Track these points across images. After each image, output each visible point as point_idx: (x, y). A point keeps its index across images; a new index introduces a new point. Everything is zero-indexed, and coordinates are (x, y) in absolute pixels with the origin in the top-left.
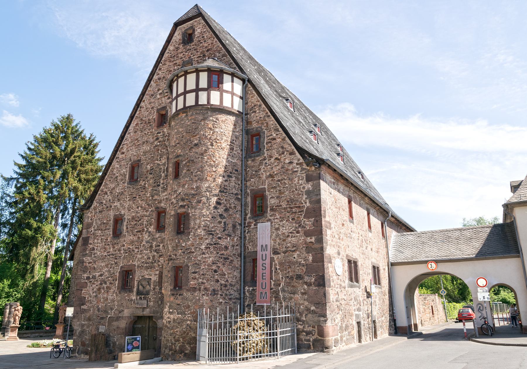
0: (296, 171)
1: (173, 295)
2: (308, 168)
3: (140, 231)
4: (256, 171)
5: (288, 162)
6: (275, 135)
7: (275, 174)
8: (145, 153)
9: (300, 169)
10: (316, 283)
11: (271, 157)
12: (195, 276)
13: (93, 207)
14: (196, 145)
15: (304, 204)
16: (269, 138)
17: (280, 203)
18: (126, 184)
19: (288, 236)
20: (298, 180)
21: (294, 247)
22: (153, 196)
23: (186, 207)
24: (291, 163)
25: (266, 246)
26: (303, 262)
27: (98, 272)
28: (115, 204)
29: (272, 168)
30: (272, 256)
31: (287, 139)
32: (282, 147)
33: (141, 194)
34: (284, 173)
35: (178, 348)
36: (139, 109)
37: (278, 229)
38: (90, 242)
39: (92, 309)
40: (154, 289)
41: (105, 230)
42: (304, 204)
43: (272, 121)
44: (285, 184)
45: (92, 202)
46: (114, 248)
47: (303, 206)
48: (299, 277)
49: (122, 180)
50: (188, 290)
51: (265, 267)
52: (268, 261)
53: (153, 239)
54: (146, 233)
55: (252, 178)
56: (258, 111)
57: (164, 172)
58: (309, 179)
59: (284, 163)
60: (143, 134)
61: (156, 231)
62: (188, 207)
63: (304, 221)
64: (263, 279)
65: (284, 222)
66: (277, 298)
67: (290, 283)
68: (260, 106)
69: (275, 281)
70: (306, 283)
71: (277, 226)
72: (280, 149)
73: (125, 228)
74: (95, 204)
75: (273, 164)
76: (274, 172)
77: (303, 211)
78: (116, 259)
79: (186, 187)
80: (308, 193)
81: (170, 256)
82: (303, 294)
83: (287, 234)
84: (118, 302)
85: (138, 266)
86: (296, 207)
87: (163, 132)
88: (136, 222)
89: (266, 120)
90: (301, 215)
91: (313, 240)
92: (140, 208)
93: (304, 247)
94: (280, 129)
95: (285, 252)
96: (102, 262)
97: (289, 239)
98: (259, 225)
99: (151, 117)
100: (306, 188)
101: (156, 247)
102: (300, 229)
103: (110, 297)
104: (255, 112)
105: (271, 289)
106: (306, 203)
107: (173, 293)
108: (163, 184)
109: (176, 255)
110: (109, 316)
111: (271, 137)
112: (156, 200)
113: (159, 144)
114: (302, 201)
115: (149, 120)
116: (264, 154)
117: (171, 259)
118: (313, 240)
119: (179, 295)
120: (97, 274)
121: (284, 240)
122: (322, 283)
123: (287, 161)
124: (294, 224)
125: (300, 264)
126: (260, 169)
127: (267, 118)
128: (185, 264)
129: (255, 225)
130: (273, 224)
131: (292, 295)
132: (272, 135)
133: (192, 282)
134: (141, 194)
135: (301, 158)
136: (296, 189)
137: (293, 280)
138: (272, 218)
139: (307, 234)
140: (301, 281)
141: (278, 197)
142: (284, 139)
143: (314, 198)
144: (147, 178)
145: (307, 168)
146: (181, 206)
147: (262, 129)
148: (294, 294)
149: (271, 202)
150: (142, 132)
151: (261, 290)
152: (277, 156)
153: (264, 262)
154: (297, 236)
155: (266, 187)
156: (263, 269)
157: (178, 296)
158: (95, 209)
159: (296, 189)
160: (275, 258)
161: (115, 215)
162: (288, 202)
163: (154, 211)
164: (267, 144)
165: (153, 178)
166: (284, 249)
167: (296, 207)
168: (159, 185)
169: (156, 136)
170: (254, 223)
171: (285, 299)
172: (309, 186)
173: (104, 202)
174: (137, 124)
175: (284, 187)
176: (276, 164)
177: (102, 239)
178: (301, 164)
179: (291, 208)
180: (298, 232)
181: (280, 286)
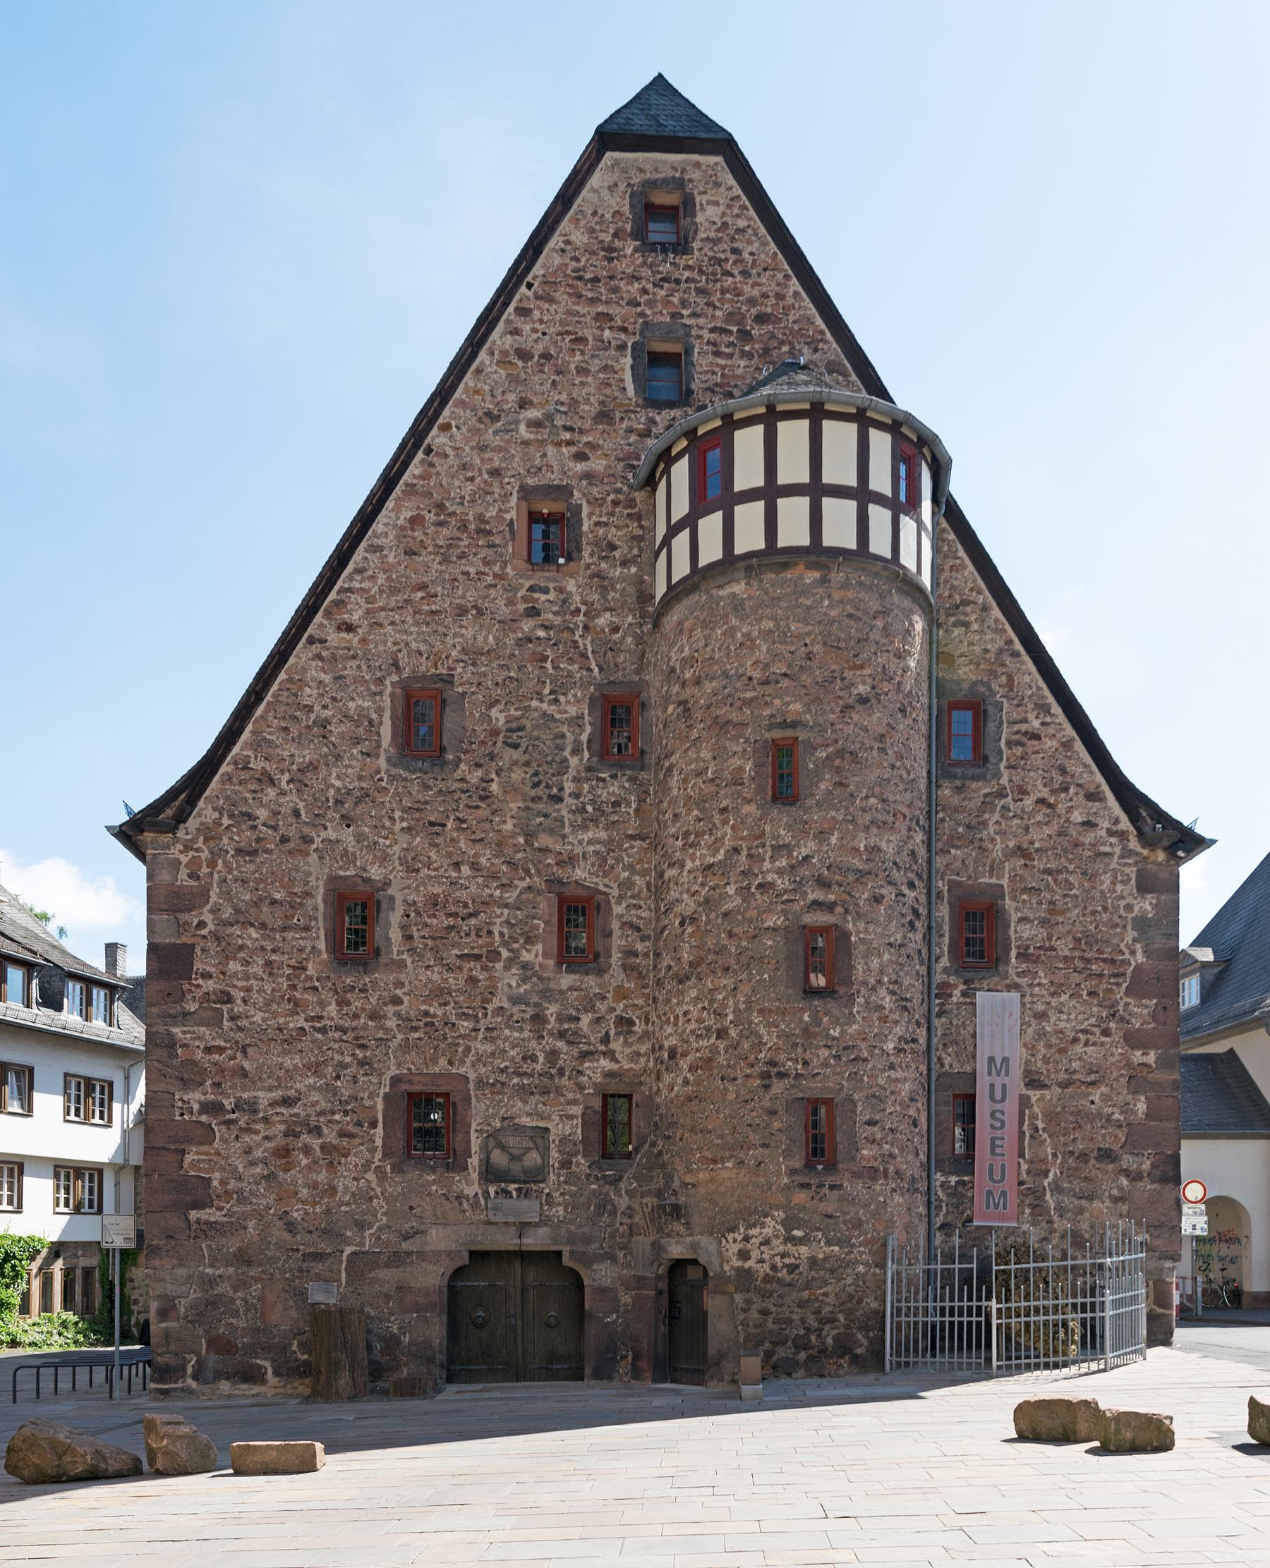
0: (1107, 854)
2: (1145, 852)
3: (477, 957)
4: (969, 827)
5: (1080, 820)
6: (1036, 724)
7: (1037, 850)
8: (472, 654)
9: (1118, 850)
10: (1157, 1173)
11: (1022, 791)
12: (873, 1134)
13: (192, 823)
15: (1127, 956)
16: (1016, 728)
17: (1050, 939)
18: (382, 762)
19: (1075, 1040)
20: (1113, 883)
21: (1091, 1072)
22: (530, 836)
24: (1089, 825)
25: (1005, 1060)
26: (1116, 1116)
27: (270, 1089)
28: (331, 834)
29: (1027, 829)
30: (1024, 1091)
31: (1079, 746)
32: (1063, 770)
33: (471, 816)
34: (1065, 850)
36: (420, 455)
37: (1042, 1016)
38: (198, 966)
39: (251, 1224)
40: (566, 1164)
41: (284, 929)
42: (1127, 956)
44: (1070, 886)
45: (192, 802)
46: (342, 1003)
47: (1123, 961)
48: (1106, 1155)
49: (356, 741)
51: (1003, 1123)
52: (1010, 1107)
53: (547, 994)
54: (507, 968)
55: (957, 847)
56: (975, 627)
57: (576, 751)
58: (1145, 885)
59: (1067, 820)
61: (559, 964)
63: (1127, 1004)
64: (993, 1153)
65: (1064, 998)
66: (1038, 1207)
67: (1077, 1169)
68: (985, 608)
69: (1031, 1162)
70: (1127, 1173)
71: (1040, 1007)
73: (395, 935)
74: (205, 812)
75: (1031, 815)
76: (1032, 843)
77: (1124, 974)
78: (363, 1047)
80: (1141, 924)
82: (1115, 1200)
83: (1071, 1035)
84: (391, 1200)
85: (481, 1083)
86: (1104, 961)
87: (561, 590)
88: (451, 921)
89: (1004, 665)
90: (1119, 985)
91: (1151, 1058)
92: (466, 870)
93: (1122, 1075)
94: (1056, 709)
95: (1059, 1085)
96: (285, 1053)
97: (1079, 1049)
98: (980, 995)
99: (492, 512)
100: (1136, 908)
101: (560, 1020)
102: (1112, 1025)
103: (345, 1182)
104: (967, 625)
105: (1021, 1183)
106: (1133, 953)
108: (576, 795)
110: (348, 1250)
111: (1024, 727)
112: (545, 851)
113: (541, 633)
114: (1122, 946)
115: (480, 518)
116: (998, 775)
118: (1151, 1058)
120: (264, 1098)
121: (1062, 1051)
122: (1171, 1174)
123: (1077, 817)
124: (1095, 1009)
125: (1108, 1120)
126: (984, 824)
127: (1008, 660)
128: (844, 1094)
129: (964, 994)
130: (1028, 999)
131: (1084, 1203)
132: (1025, 721)
133: (865, 1152)
134: (471, 816)
135: (1124, 818)
136: (1105, 909)
137: (1087, 1162)
138: (1023, 981)
139: (1134, 1040)
140: (1111, 1167)
141: (1043, 922)
142: (1067, 745)
143: (1159, 943)
144: (492, 757)
145: (1139, 849)
147: (993, 694)
148: (1090, 1198)
149: (1021, 931)
150: (446, 560)
151: (989, 1185)
152: (1044, 793)
153: (998, 1107)
154: (1103, 1044)
155: (1005, 882)
156: (992, 1127)
158: (209, 833)
159: (1105, 909)
160: (1033, 1099)
161: (333, 879)
162: (1078, 940)
163: (539, 892)
164: (1009, 744)
165: (527, 764)
166: (1062, 1076)
167: (1104, 961)
168: (558, 799)
170: (962, 987)
171: (1061, 1210)
172: (1146, 905)
173: (263, 814)
174: (416, 521)
175: (1065, 896)
176: (1039, 818)
177: (269, 964)
178: (1122, 835)
179: (1088, 961)
180: (1106, 1032)
181: (1047, 1176)
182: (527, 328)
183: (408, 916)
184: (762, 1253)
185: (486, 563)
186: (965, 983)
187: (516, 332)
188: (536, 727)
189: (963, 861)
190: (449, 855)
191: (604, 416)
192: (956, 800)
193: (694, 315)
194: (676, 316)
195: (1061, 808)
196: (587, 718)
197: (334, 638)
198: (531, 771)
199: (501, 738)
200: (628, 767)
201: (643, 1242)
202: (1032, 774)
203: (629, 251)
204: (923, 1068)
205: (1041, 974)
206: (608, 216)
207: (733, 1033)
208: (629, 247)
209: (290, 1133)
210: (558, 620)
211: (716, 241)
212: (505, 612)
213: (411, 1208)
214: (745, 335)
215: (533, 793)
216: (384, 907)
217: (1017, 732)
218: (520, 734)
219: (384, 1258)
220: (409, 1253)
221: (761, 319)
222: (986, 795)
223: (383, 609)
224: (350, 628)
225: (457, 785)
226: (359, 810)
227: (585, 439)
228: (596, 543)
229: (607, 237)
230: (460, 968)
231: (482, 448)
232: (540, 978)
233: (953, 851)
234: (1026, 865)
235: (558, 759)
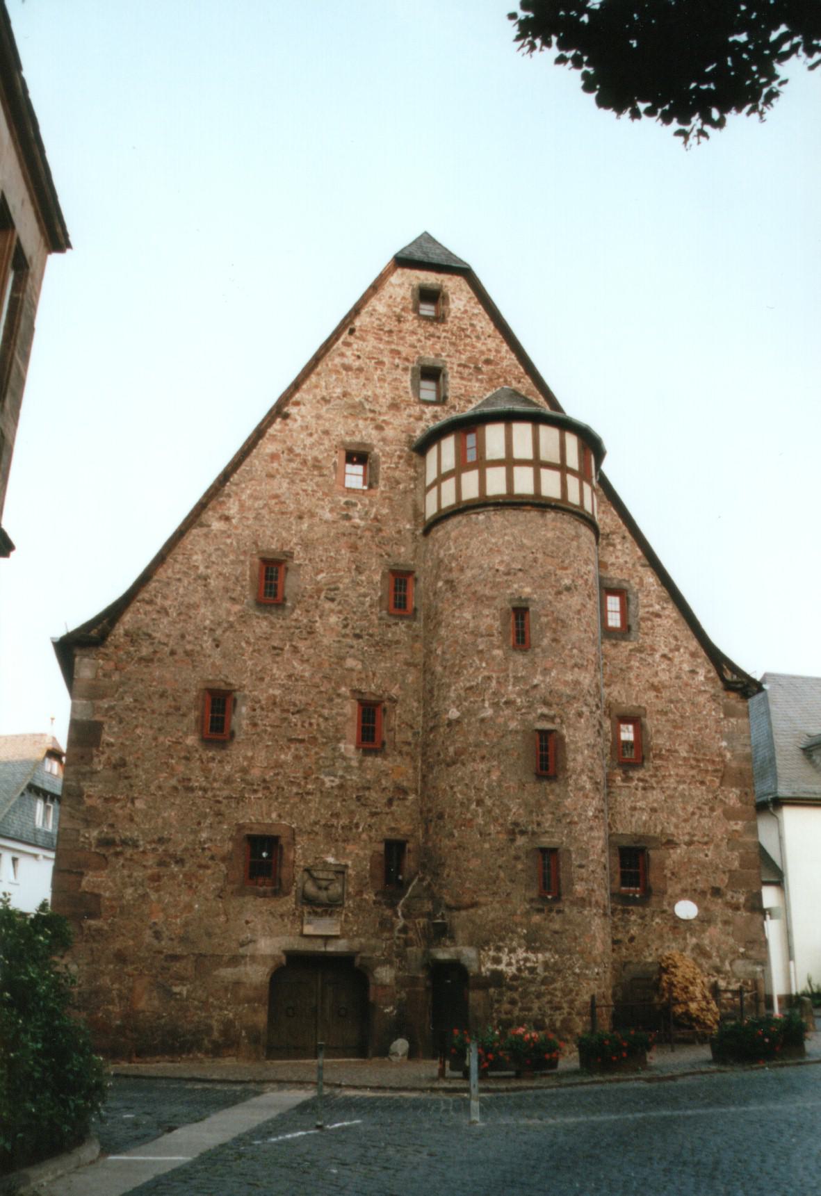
1: (540, 911)
3: (302, 741)
11: (653, 650)
14: (568, 589)
23: (558, 720)
24: (693, 672)
33: (302, 646)
35: (558, 1024)
43: (651, 579)
46: (206, 771)
50: (573, 903)
56: (619, 547)
60: (298, 487)
72: (671, 640)
75: (659, 665)
89: (636, 571)
104: (614, 545)
107: (536, 905)
109: (539, 824)
111: (651, 610)
115: (316, 459)
119: (559, 912)
123: (686, 667)
129: (623, 780)
136: (706, 727)
150: (292, 482)
152: (666, 651)
157: (553, 914)
162: (691, 746)
163: (346, 698)
165: (340, 612)
176: (663, 666)
179: (698, 761)
182: (349, 353)
185: (318, 485)
187: (342, 355)
188: (347, 588)
190: (285, 670)
191: (394, 406)
193: (448, 356)
194: (437, 355)
195: (676, 661)
197: (217, 525)
198: (342, 617)
199: (323, 595)
200: (407, 617)
201: (415, 951)
203: (410, 318)
206: (399, 300)
207: (488, 802)
208: (410, 316)
209: (162, 864)
210: (362, 523)
211: (461, 319)
212: (328, 516)
213: (247, 922)
214: (478, 370)
215: (343, 632)
216: (239, 702)
219: (226, 959)
220: (243, 957)
221: (488, 362)
224: (227, 519)
227: (382, 418)
228: (388, 479)
229: (398, 310)
230: (289, 748)
231: (318, 417)
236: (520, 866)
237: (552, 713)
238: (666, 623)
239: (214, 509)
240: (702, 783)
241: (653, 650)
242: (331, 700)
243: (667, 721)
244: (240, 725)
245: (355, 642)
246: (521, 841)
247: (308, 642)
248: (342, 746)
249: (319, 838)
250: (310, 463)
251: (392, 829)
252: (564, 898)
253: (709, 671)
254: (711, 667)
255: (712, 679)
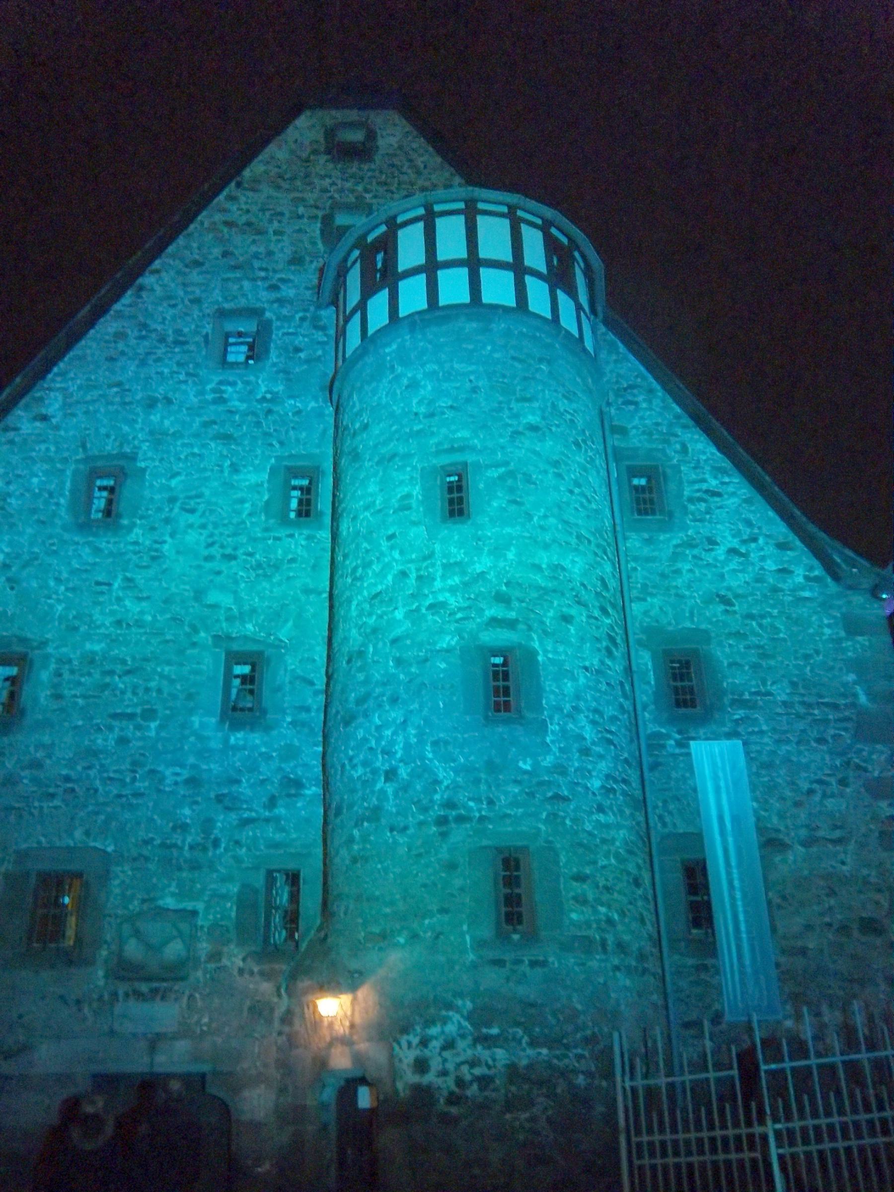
3: (131, 717)
5: (774, 568)
11: (712, 542)
16: (697, 487)
17: (764, 683)
23: (521, 626)
33: (140, 577)
44: (776, 630)
62: (530, 628)
79: (511, 555)
81: (450, 805)
111: (704, 486)
117: (460, 819)
146: (494, 622)
152: (735, 543)
162: (794, 684)
165: (203, 526)
169: (214, 391)
176: (733, 565)
179: (809, 706)
183: (60, 675)
184: (445, 1061)
186: (680, 732)
189: (661, 608)
192: (646, 551)
196: (266, 485)
202: (719, 526)
204: (642, 819)
205: (762, 720)
217: (698, 491)
218: (198, 500)
222: (676, 546)
223: (78, 402)
224: (44, 418)
225: (131, 548)
226: (24, 573)
232: (200, 738)
233: (649, 599)
234: (727, 611)
235: (235, 521)
236: (458, 882)
237: (512, 615)
238: (732, 502)
239: (27, 407)
240: (821, 741)
241: (712, 542)
242: (181, 652)
243: (748, 647)
244: (36, 700)
245: (224, 567)
246: (458, 834)
247: (151, 572)
248: (196, 720)
249: (152, 866)
250: (170, 339)
251: (276, 845)
252: (543, 934)
253: (811, 569)
254: (816, 563)
255: (817, 579)
